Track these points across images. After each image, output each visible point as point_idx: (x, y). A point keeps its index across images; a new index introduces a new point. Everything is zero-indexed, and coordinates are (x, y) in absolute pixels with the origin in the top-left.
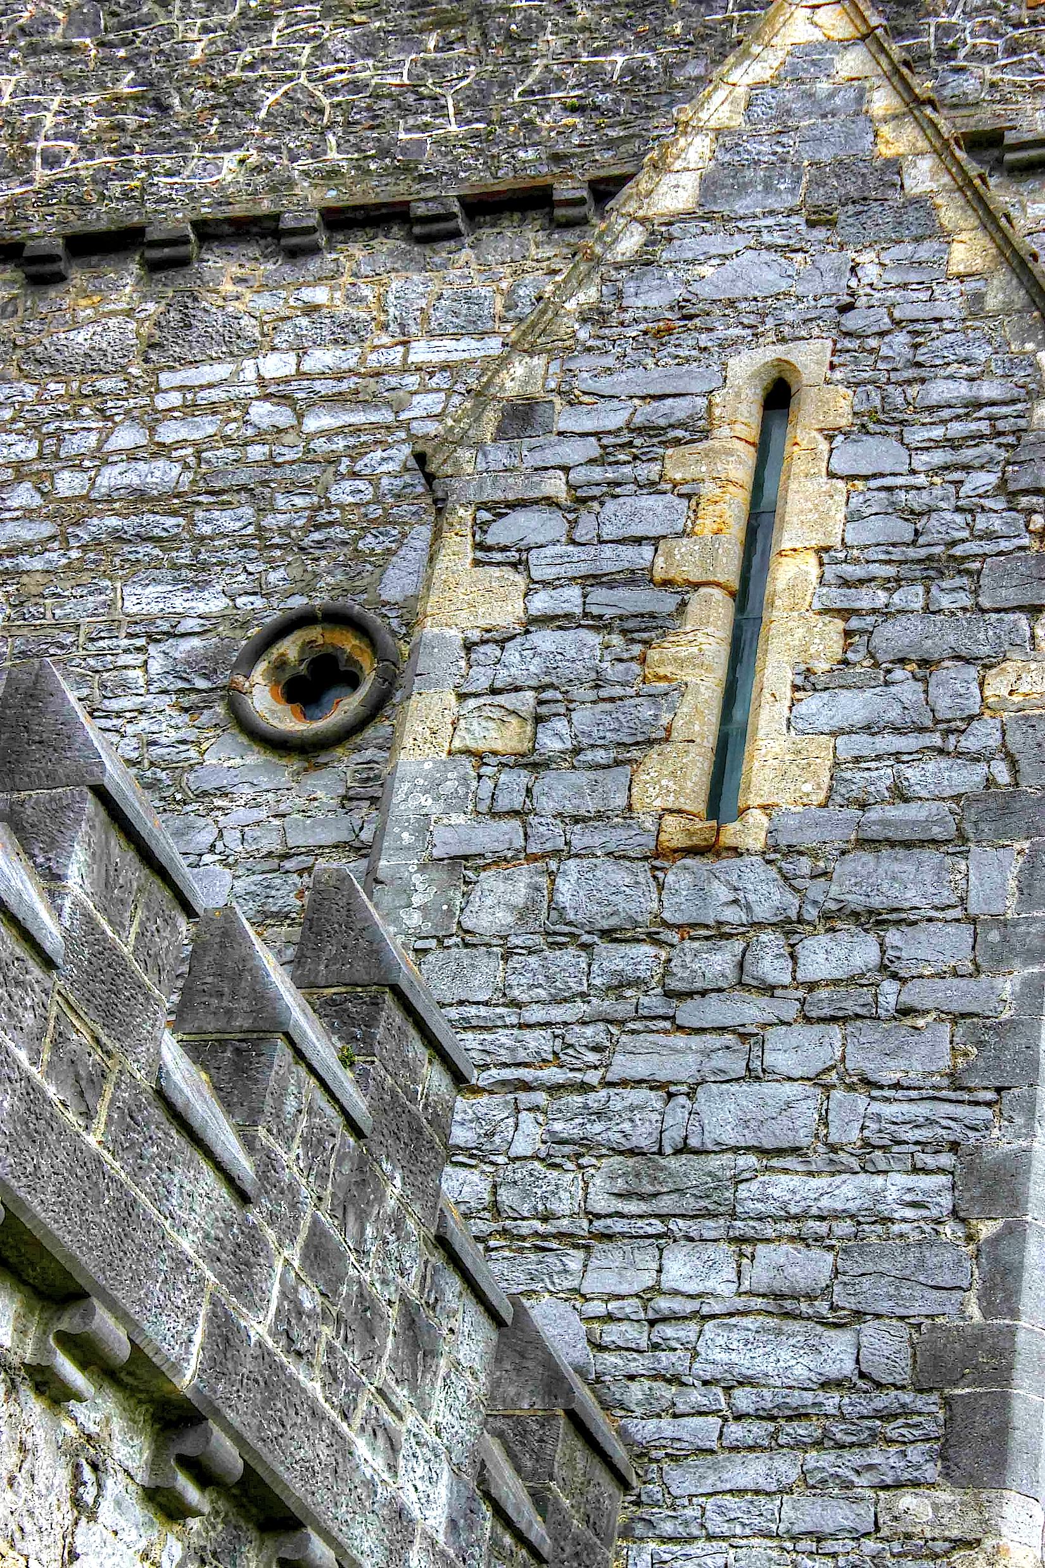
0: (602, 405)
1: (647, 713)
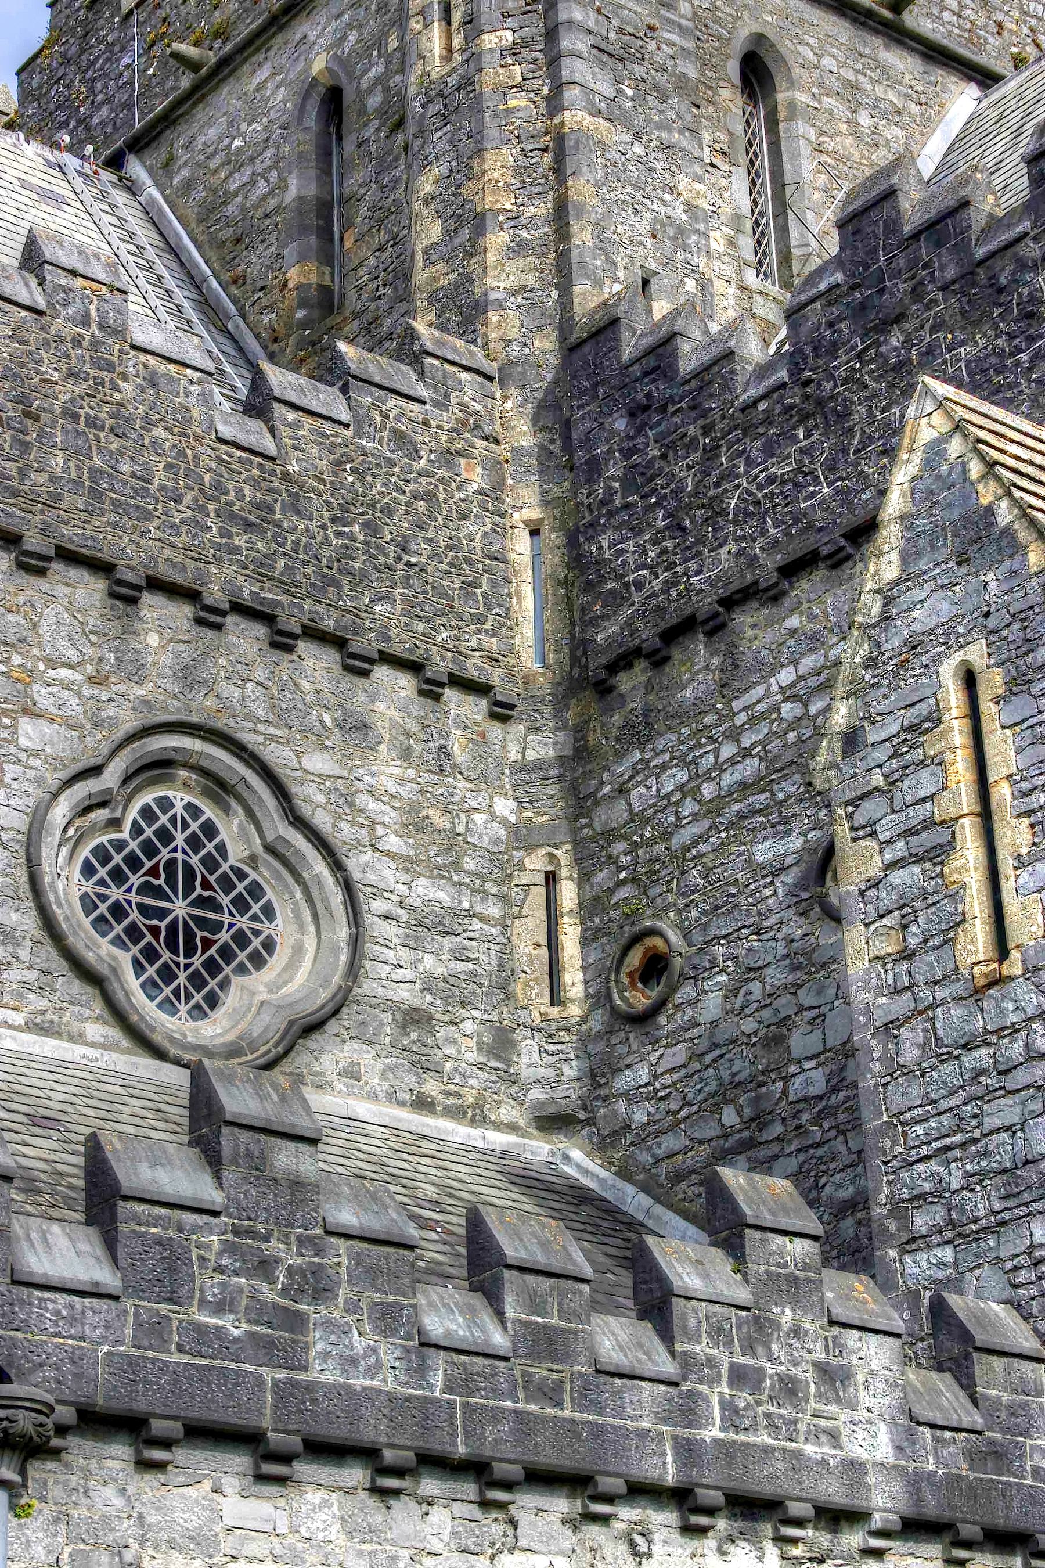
0: (888, 719)
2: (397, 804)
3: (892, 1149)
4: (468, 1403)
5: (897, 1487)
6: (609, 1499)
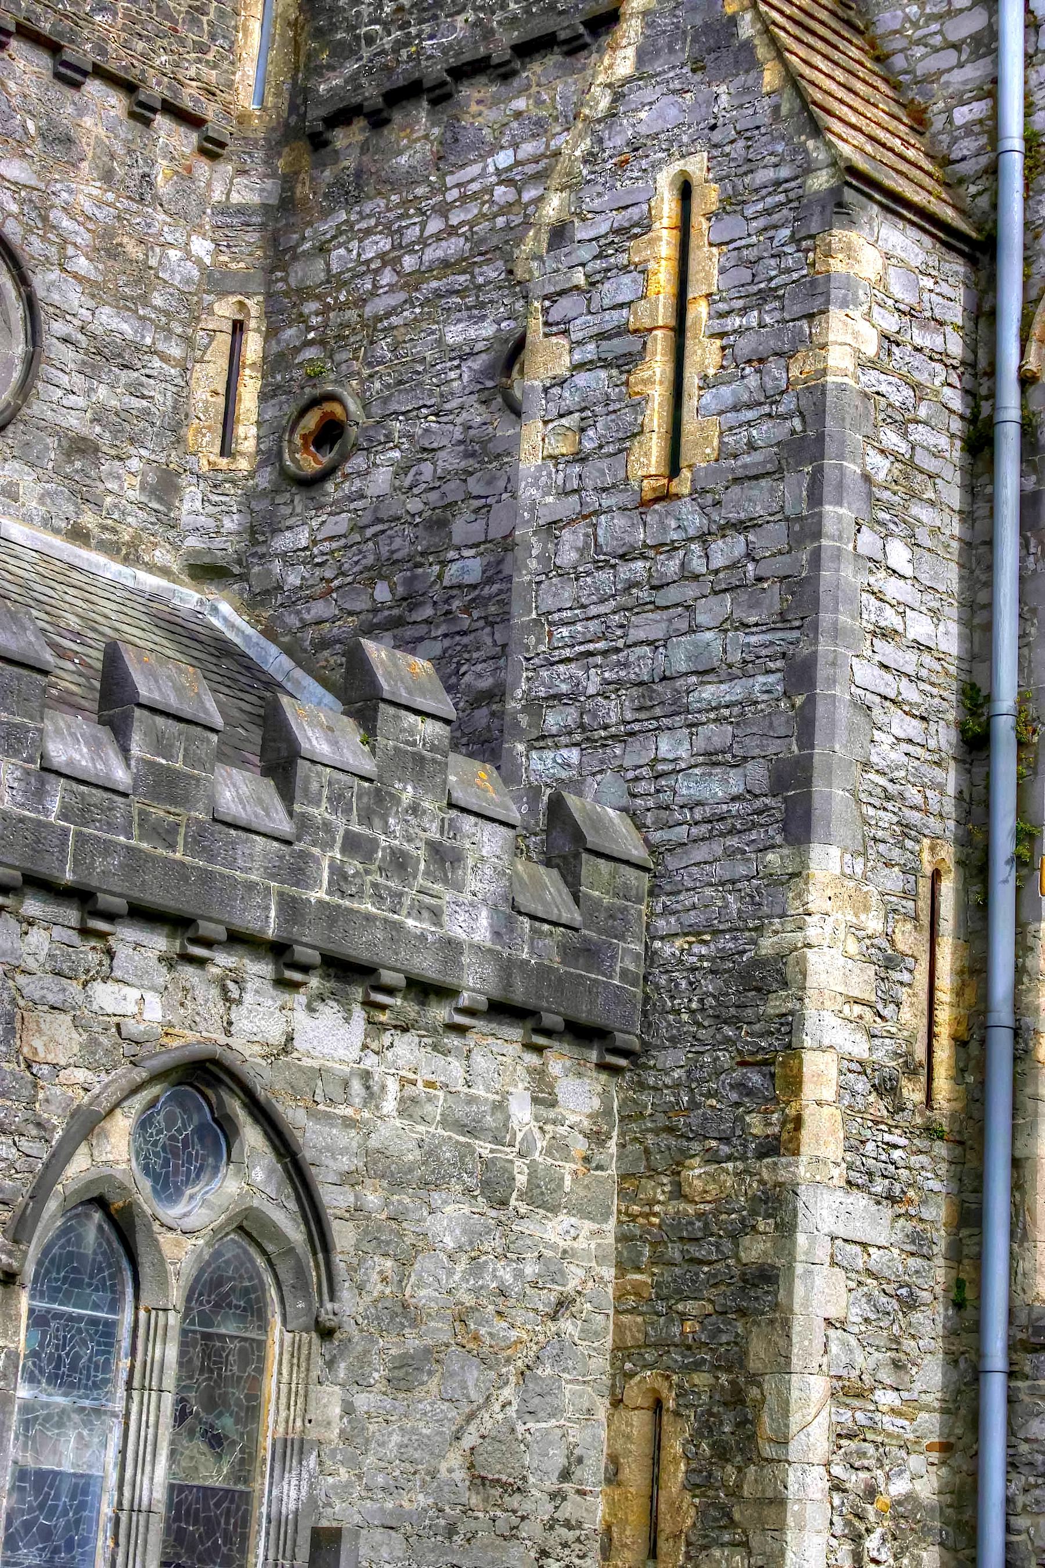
1: (629, 418)
2: (91, 226)
3: (535, 647)
4: (81, 832)
5: (489, 970)
6: (208, 943)
